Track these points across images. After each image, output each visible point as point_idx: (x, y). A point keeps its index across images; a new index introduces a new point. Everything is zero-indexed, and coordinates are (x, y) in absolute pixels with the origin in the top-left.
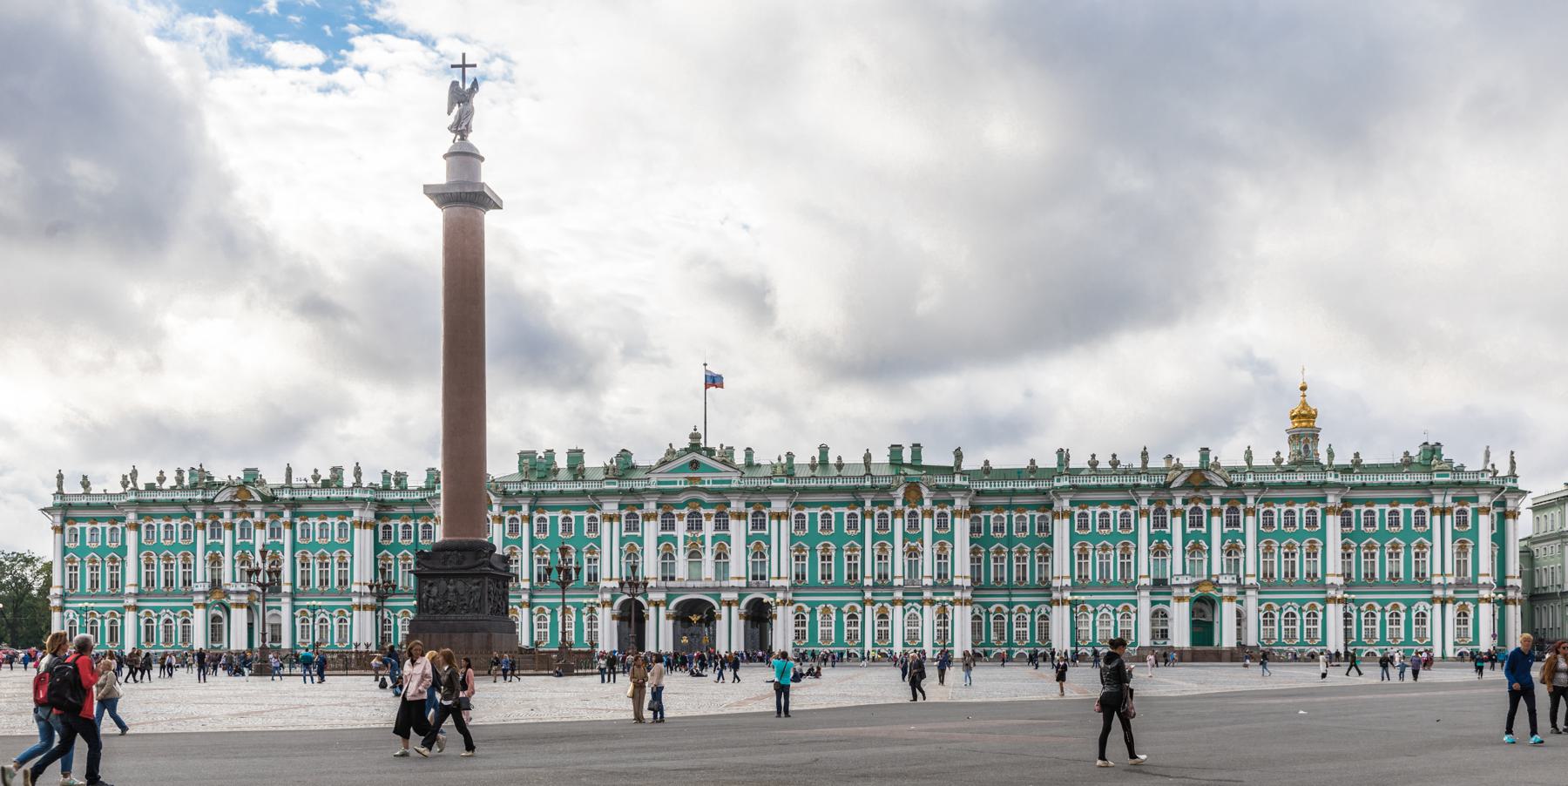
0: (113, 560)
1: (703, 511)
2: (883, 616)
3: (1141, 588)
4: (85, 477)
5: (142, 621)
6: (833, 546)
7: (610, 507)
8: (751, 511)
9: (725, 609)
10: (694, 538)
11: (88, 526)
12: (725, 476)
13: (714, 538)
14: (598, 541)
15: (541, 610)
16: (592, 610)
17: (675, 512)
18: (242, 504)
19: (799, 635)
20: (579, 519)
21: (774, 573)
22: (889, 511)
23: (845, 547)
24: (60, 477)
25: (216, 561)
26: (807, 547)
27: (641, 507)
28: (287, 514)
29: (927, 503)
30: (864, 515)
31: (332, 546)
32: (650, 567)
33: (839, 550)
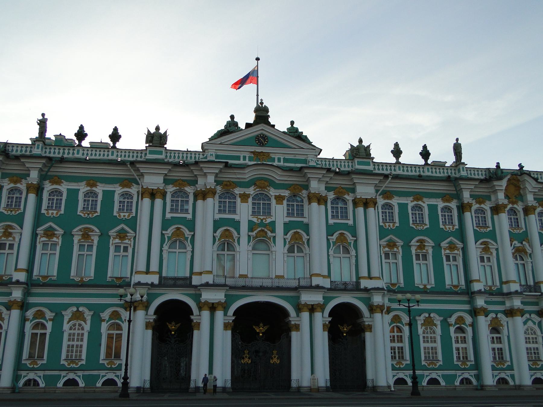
2: (495, 329)
6: (429, 243)
8: (331, 196)
9: (305, 315)
10: (262, 224)
12: (299, 154)
13: (287, 227)
14: (133, 223)
15: (40, 314)
16: (116, 315)
17: (238, 191)
19: (397, 354)
20: (109, 196)
21: (364, 272)
22: (487, 206)
23: (444, 244)
26: (400, 243)
27: (194, 182)
29: (530, 198)
30: (463, 208)
33: (437, 247)
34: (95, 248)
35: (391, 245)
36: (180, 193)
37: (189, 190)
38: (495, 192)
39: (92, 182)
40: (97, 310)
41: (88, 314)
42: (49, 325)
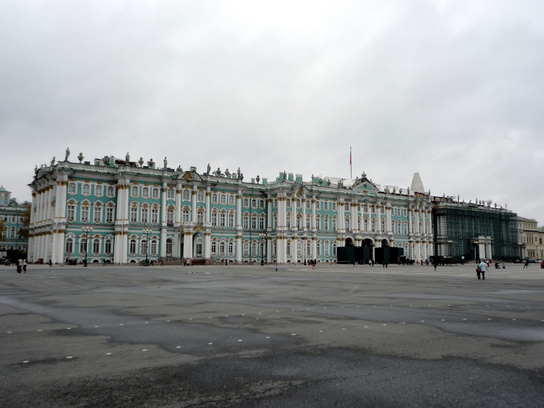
0: (98, 204)
1: (369, 204)
3: (461, 239)
4: (81, 154)
5: (130, 240)
7: (342, 200)
11: (83, 183)
14: (336, 213)
16: (335, 242)
17: (361, 204)
18: (188, 181)
24: (68, 153)
25: (171, 209)
27: (350, 200)
28: (209, 189)
30: (409, 210)
31: (227, 206)
32: (354, 226)
34: (328, 221)
35: (393, 221)
36: (347, 204)
37: (349, 203)
38: (417, 205)
39: (327, 199)
40: (332, 240)
41: (329, 241)
42: (321, 244)
